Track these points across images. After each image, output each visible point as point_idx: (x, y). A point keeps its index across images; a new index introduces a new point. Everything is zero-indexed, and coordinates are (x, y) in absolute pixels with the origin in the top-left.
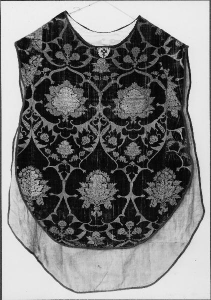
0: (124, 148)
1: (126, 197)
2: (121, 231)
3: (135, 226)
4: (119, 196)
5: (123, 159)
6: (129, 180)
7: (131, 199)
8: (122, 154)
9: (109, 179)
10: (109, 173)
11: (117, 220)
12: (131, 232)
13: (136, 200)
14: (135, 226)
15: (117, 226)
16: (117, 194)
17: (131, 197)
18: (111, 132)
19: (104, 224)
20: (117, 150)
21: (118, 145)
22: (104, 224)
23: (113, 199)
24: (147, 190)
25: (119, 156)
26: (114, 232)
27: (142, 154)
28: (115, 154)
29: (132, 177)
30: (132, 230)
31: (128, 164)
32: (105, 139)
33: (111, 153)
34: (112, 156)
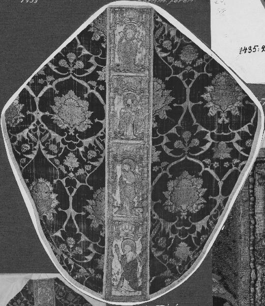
0: (179, 52)
1: (182, 105)
2: (177, 144)
3: (192, 137)
4: (175, 105)
5: (178, 64)
6: (186, 86)
7: (188, 108)
8: (177, 58)
9: (164, 86)
10: (163, 80)
11: (173, 130)
12: (188, 145)
13: (194, 108)
14: (192, 137)
15: (173, 138)
16: (173, 102)
17: (188, 104)
18: (165, 35)
19: (160, 135)
20: (171, 55)
21: (172, 49)
22: (160, 135)
23: (169, 108)
24: (204, 96)
25: (175, 61)
26: (169, 145)
27: (199, 58)
28: (171, 59)
29: (188, 83)
30: (190, 142)
31: (184, 69)
32: (159, 43)
33: (165, 58)
34: (167, 61)
